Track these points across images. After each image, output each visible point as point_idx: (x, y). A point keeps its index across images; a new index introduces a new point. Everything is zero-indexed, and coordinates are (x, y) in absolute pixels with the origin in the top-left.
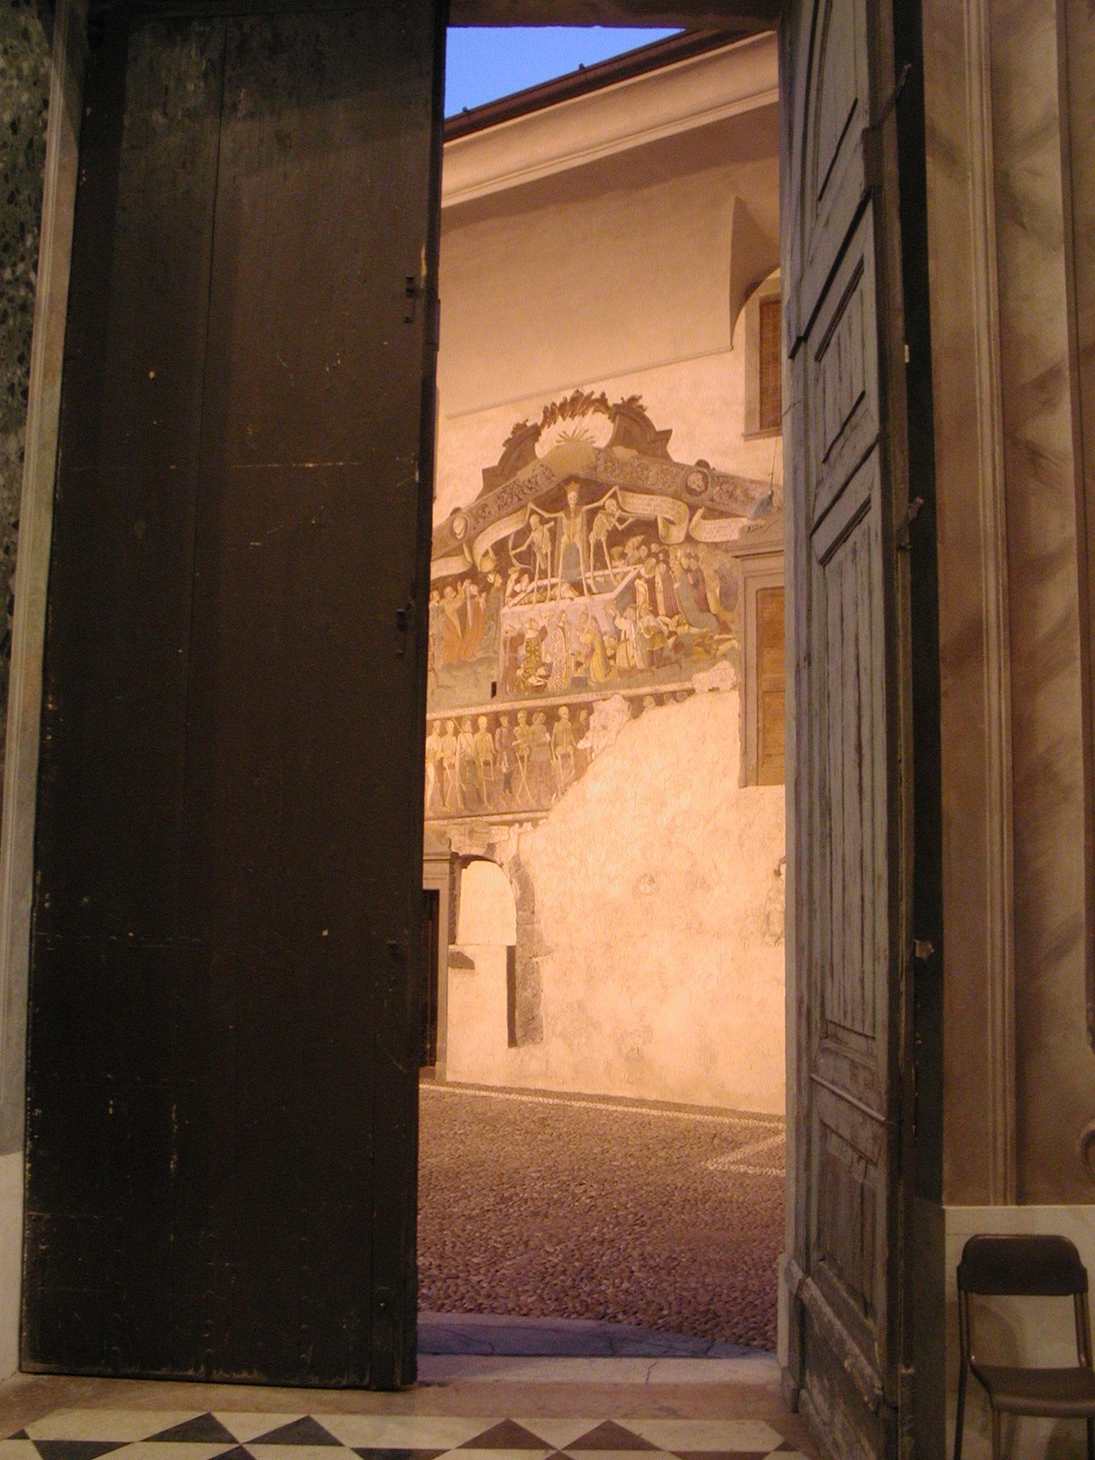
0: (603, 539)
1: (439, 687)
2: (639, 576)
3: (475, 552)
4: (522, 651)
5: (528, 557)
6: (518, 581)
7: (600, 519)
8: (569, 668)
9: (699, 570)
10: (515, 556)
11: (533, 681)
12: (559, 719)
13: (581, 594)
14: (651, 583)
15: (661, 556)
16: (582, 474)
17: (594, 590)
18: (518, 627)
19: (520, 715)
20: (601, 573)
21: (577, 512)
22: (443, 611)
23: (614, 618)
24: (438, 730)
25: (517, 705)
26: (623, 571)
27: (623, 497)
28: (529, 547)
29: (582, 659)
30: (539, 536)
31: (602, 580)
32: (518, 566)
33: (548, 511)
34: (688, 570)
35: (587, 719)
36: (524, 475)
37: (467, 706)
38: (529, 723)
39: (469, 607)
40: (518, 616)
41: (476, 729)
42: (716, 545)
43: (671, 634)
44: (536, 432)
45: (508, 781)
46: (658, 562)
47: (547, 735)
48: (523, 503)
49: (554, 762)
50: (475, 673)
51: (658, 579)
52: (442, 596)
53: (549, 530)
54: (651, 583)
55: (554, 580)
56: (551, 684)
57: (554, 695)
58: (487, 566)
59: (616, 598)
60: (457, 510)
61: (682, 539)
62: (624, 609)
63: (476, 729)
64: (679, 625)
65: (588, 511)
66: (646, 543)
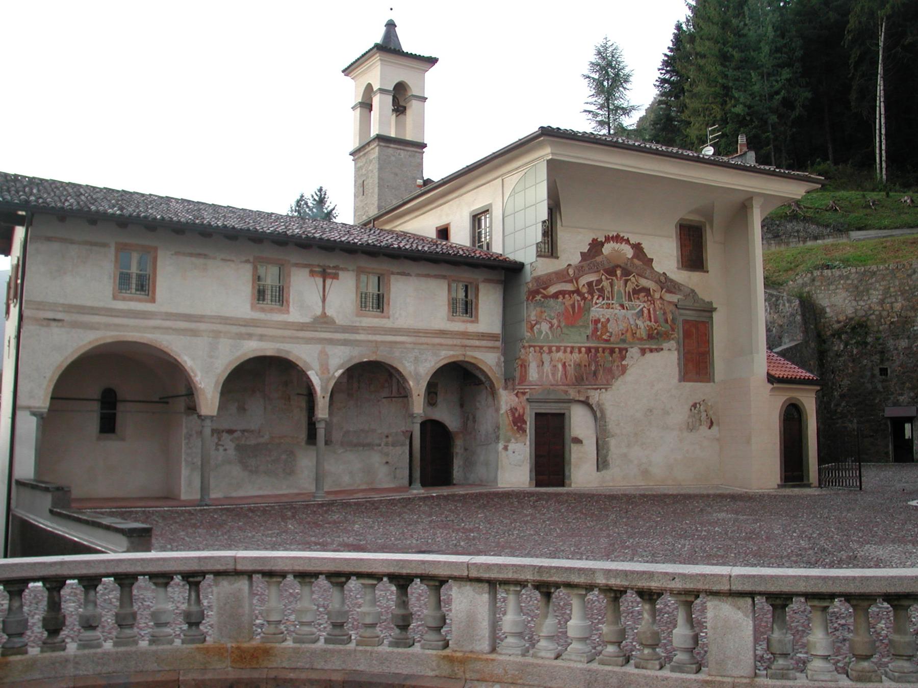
4: (599, 325)
5: (602, 290)
11: (604, 337)
14: (649, 310)
16: (622, 265)
21: (621, 279)
30: (606, 284)
36: (599, 259)
38: (603, 352)
40: (598, 311)
41: (580, 352)
42: (670, 302)
44: (602, 244)
45: (595, 374)
54: (649, 310)
56: (612, 339)
58: (585, 290)
60: (569, 265)
63: (580, 352)
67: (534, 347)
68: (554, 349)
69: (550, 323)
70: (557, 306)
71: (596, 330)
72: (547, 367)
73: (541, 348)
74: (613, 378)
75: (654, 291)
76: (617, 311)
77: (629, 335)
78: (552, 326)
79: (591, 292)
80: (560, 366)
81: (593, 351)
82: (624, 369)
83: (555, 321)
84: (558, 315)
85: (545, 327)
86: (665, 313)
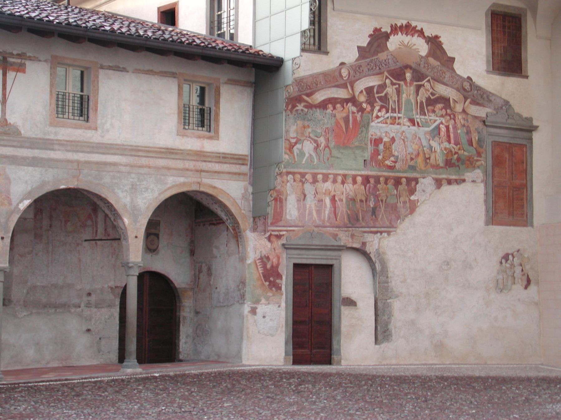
0: (424, 101)
1: (331, 157)
2: (442, 123)
3: (355, 89)
4: (381, 147)
5: (384, 100)
6: (379, 111)
7: (422, 90)
8: (407, 160)
9: (468, 126)
10: (378, 97)
11: (388, 163)
12: (401, 184)
13: (414, 125)
14: (447, 128)
15: (452, 116)
17: (420, 124)
18: (379, 134)
19: (381, 179)
20: (423, 117)
21: (411, 84)
22: (335, 116)
23: (429, 140)
24: (331, 180)
25: (380, 174)
26: (435, 119)
27: (434, 83)
28: (386, 95)
29: (414, 157)
30: (390, 90)
31: (424, 121)
32: (380, 103)
33: (395, 79)
34: (464, 126)
35: (415, 186)
37: (351, 170)
38: (386, 183)
39: (351, 118)
40: (379, 127)
41: (355, 182)
42: (476, 117)
43: (456, 153)
46: (451, 118)
47: (395, 191)
48: (382, 71)
49: (399, 204)
50: (354, 153)
51: (451, 127)
52: (334, 108)
53: (396, 89)
54: (447, 128)
55: (399, 115)
56: (398, 166)
57: (399, 172)
58: (362, 98)
59: (431, 131)
61: (461, 110)
62: (434, 137)
63: (355, 182)
64: (459, 149)
65: (417, 85)
66: (445, 108)
67: (293, 174)
68: (320, 177)
69: (316, 141)
70: (326, 120)
71: (376, 152)
72: (311, 202)
73: (303, 175)
74: (398, 218)
75: (455, 101)
76: (404, 128)
77: (420, 160)
78: (318, 146)
79: (371, 101)
80: (328, 201)
81: (372, 181)
82: (412, 208)
83: (322, 140)
84: (327, 131)
85: (308, 147)
86: (468, 132)
